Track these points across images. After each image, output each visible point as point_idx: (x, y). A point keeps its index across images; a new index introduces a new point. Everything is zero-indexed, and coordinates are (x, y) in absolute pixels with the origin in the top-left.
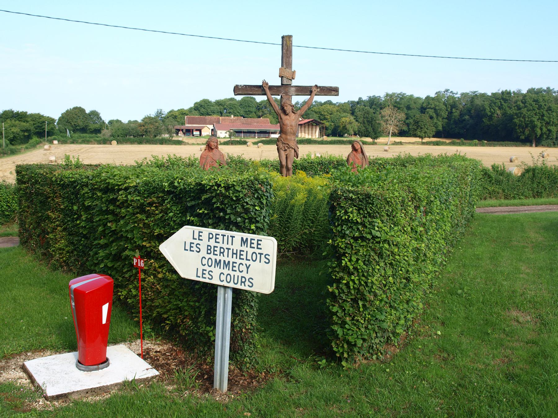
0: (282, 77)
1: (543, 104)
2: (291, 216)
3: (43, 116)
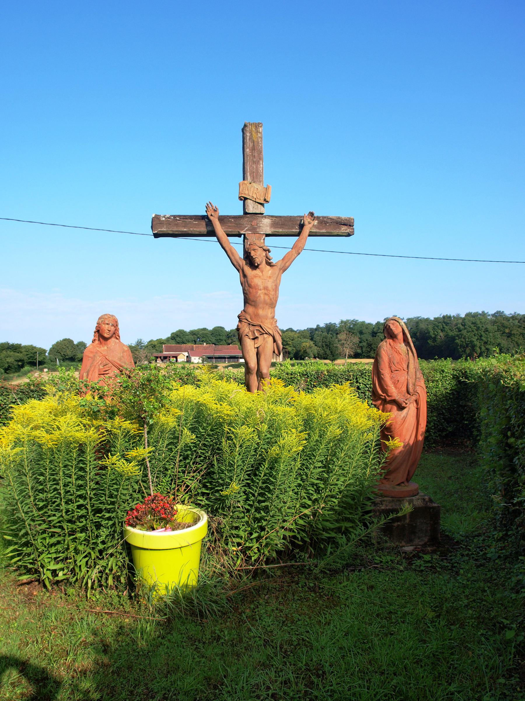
0: (244, 199)
1: (480, 326)
2: (272, 483)
3: (35, 347)
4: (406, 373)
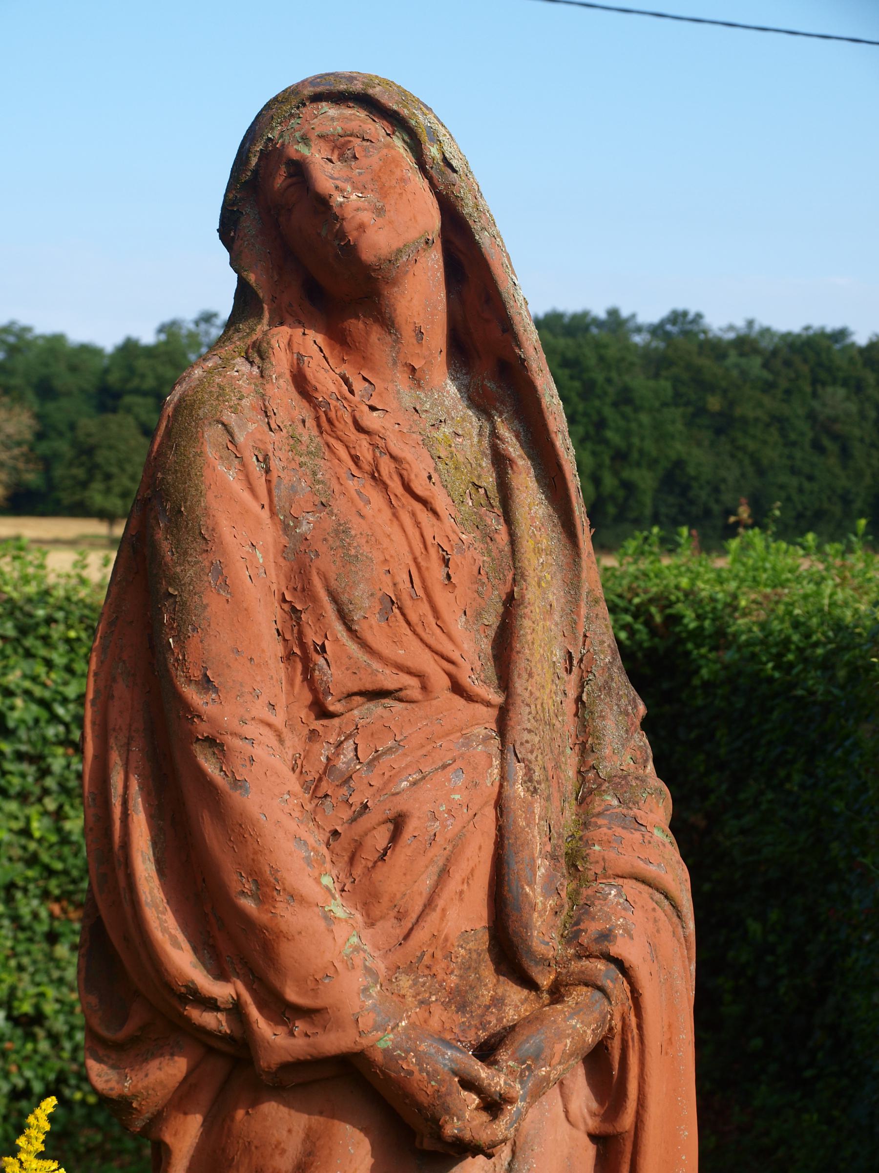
4: (492, 714)
